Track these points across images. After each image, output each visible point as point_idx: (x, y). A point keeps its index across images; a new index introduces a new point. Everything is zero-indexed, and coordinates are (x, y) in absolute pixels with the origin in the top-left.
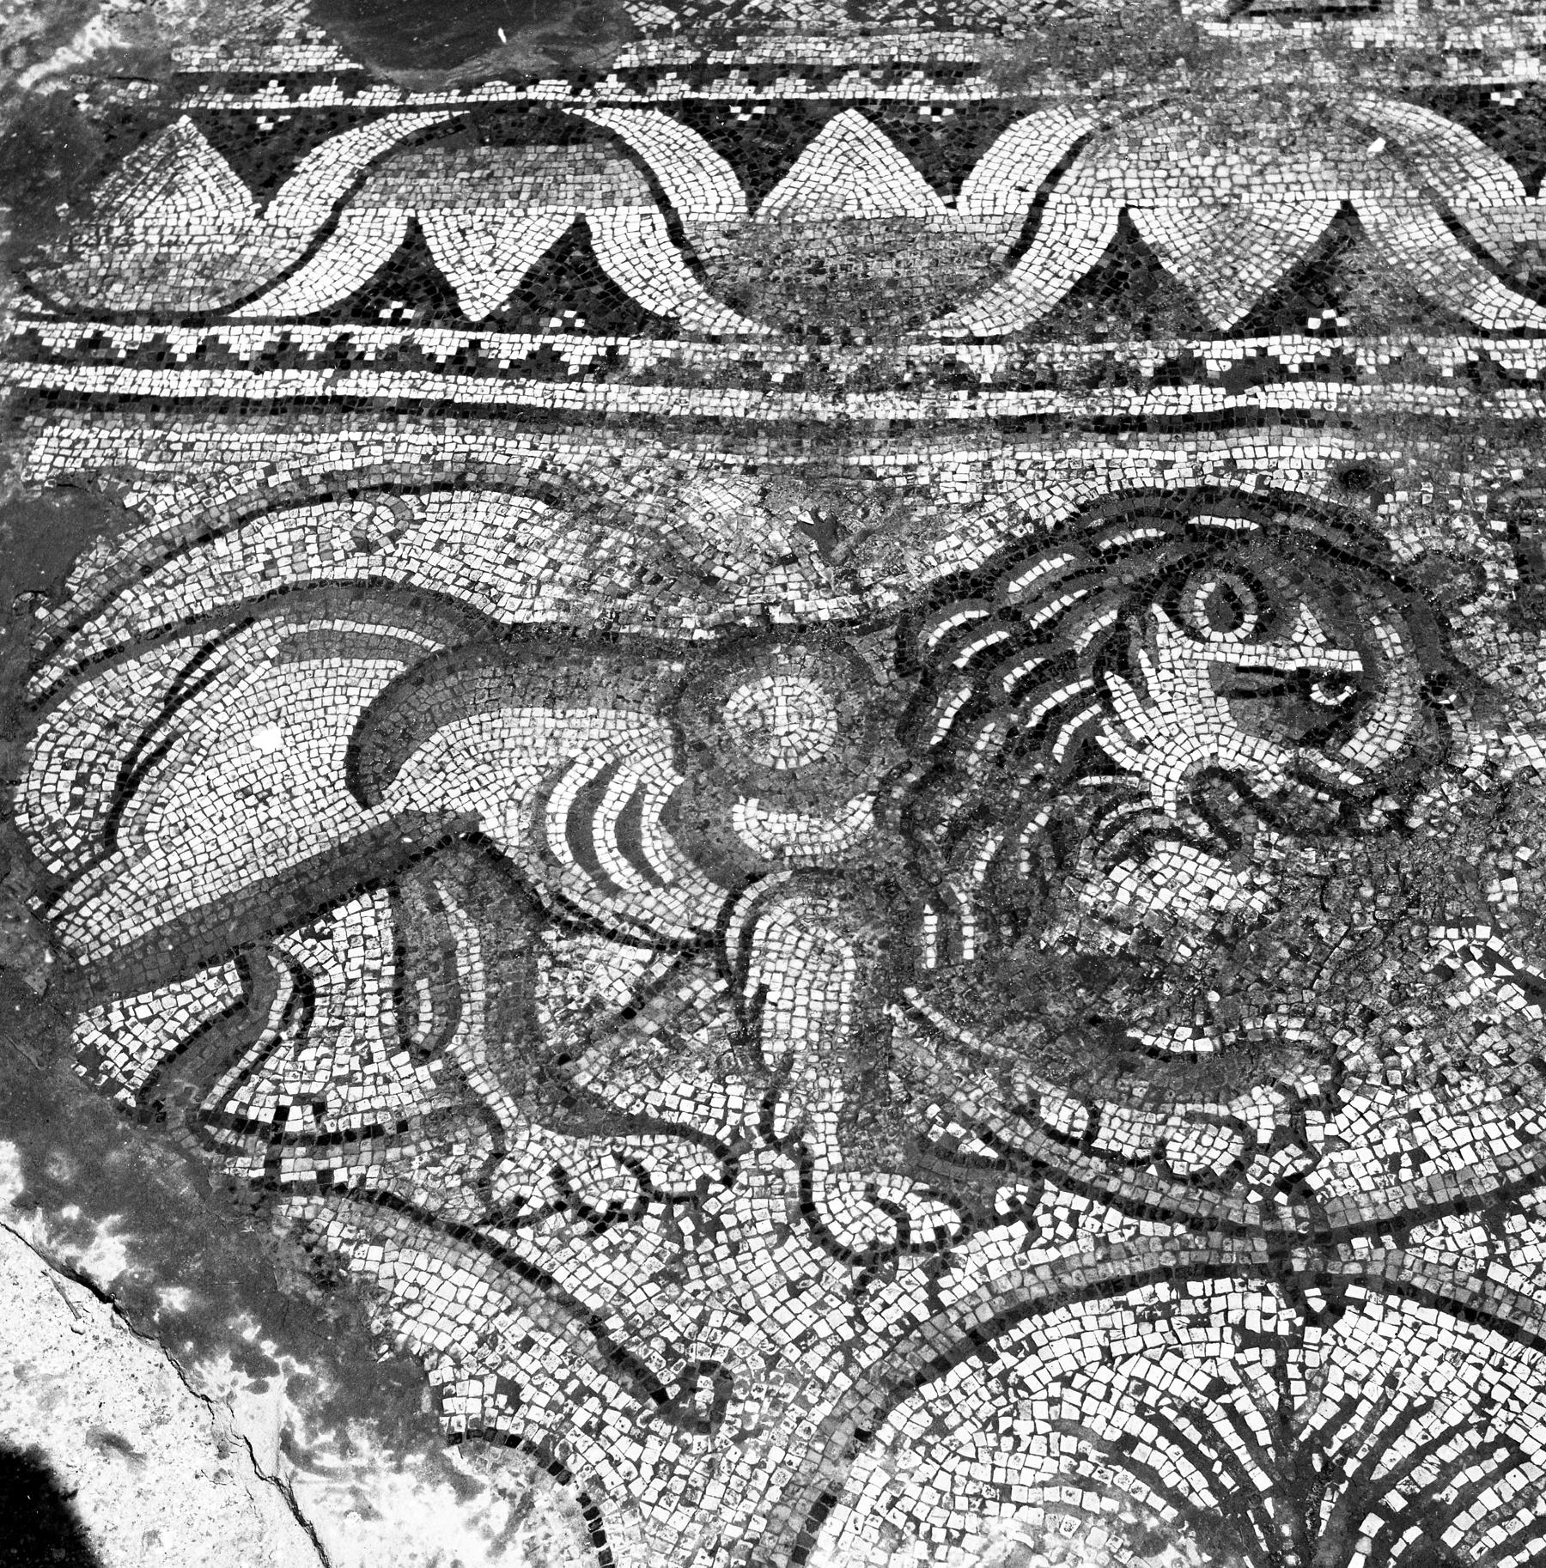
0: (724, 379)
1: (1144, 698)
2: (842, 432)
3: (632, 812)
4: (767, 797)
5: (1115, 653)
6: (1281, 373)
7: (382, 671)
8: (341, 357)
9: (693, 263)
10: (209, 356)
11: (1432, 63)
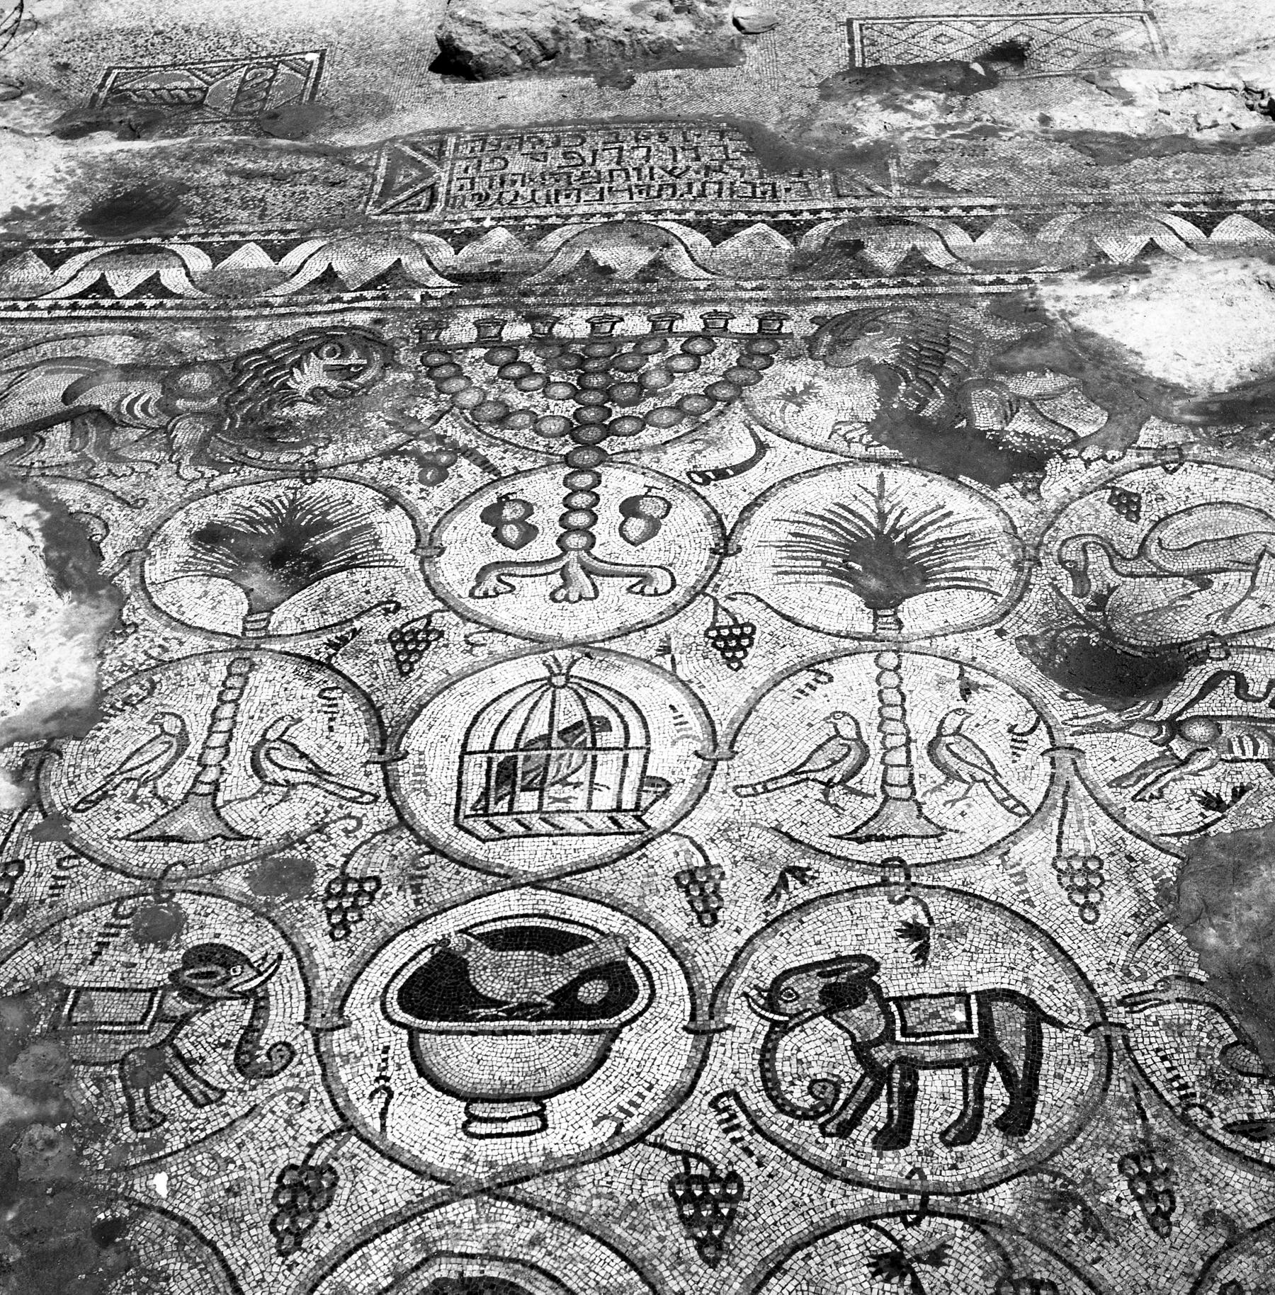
0: (195, 308)
1: (303, 372)
2: (230, 317)
3: (148, 401)
4: (187, 399)
5: (298, 364)
6: (365, 299)
7: (76, 376)
8: (74, 307)
9: (192, 281)
10: (31, 308)
11: (439, 223)
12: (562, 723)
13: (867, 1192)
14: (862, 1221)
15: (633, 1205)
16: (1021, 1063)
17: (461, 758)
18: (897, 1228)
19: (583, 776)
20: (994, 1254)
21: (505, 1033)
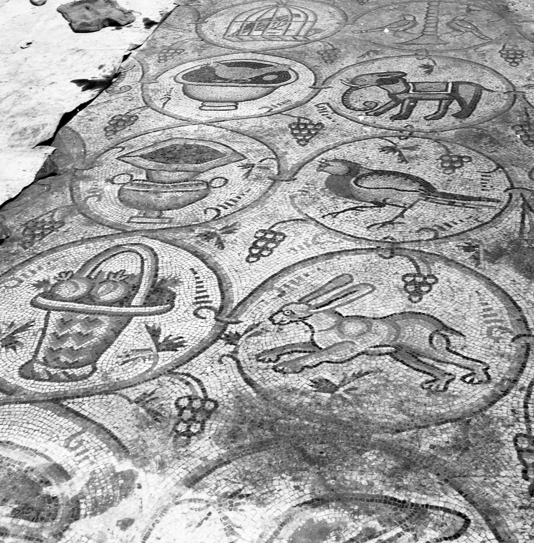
12: (279, 14)
13: (383, 130)
14: (379, 138)
15: (272, 129)
16: (469, 101)
17: (231, 23)
18: (396, 140)
19: (284, 28)
20: (442, 149)
21: (227, 86)
